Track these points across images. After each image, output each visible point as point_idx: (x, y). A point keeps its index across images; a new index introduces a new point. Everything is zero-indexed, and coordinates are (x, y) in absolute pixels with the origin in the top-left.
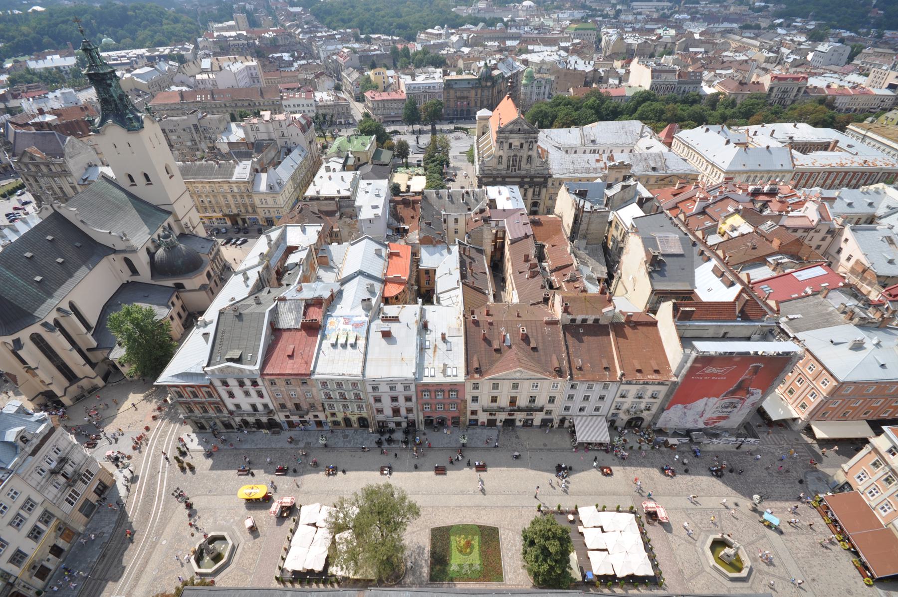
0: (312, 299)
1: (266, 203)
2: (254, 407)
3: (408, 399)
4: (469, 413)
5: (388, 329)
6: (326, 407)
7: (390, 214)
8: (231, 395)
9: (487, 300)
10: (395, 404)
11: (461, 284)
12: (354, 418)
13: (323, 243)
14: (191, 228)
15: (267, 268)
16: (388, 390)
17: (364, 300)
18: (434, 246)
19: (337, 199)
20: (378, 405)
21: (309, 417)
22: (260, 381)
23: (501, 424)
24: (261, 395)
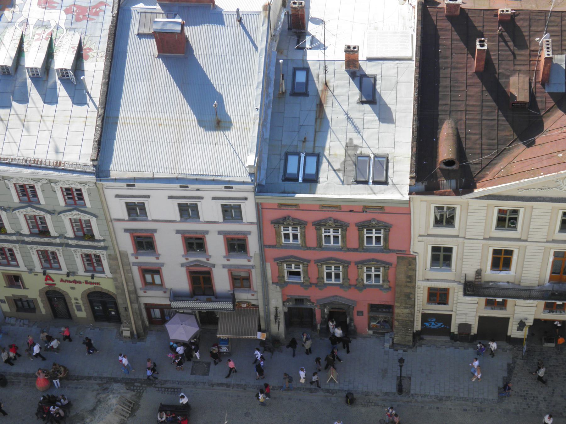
4: (421, 296)
20: (147, 259)
23: (523, 334)
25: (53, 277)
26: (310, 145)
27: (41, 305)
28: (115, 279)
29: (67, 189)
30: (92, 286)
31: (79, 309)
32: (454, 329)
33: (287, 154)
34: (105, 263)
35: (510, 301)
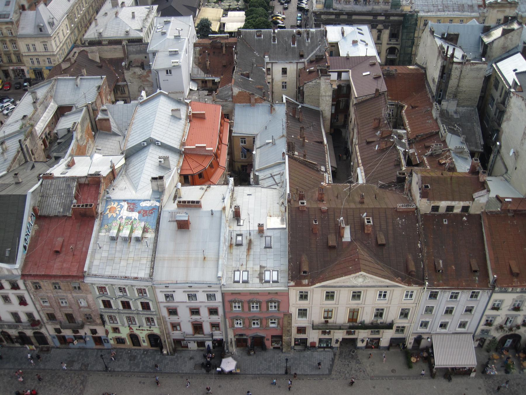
0: (86, 177)
1: (35, 49)
3: (213, 311)
4: (294, 331)
5: (186, 219)
6: (106, 319)
7: (194, 62)
9: (323, 179)
10: (195, 317)
11: (287, 157)
12: (142, 335)
13: (104, 101)
16: (186, 299)
17: (154, 179)
19: (124, 43)
20: (174, 319)
21: (85, 331)
22: (21, 283)
23: (338, 345)
25: (133, 328)
27: (127, 340)
28: (160, 328)
29: (139, 289)
32: (308, 344)
33: (234, 271)
34: (156, 321)
35: (332, 331)
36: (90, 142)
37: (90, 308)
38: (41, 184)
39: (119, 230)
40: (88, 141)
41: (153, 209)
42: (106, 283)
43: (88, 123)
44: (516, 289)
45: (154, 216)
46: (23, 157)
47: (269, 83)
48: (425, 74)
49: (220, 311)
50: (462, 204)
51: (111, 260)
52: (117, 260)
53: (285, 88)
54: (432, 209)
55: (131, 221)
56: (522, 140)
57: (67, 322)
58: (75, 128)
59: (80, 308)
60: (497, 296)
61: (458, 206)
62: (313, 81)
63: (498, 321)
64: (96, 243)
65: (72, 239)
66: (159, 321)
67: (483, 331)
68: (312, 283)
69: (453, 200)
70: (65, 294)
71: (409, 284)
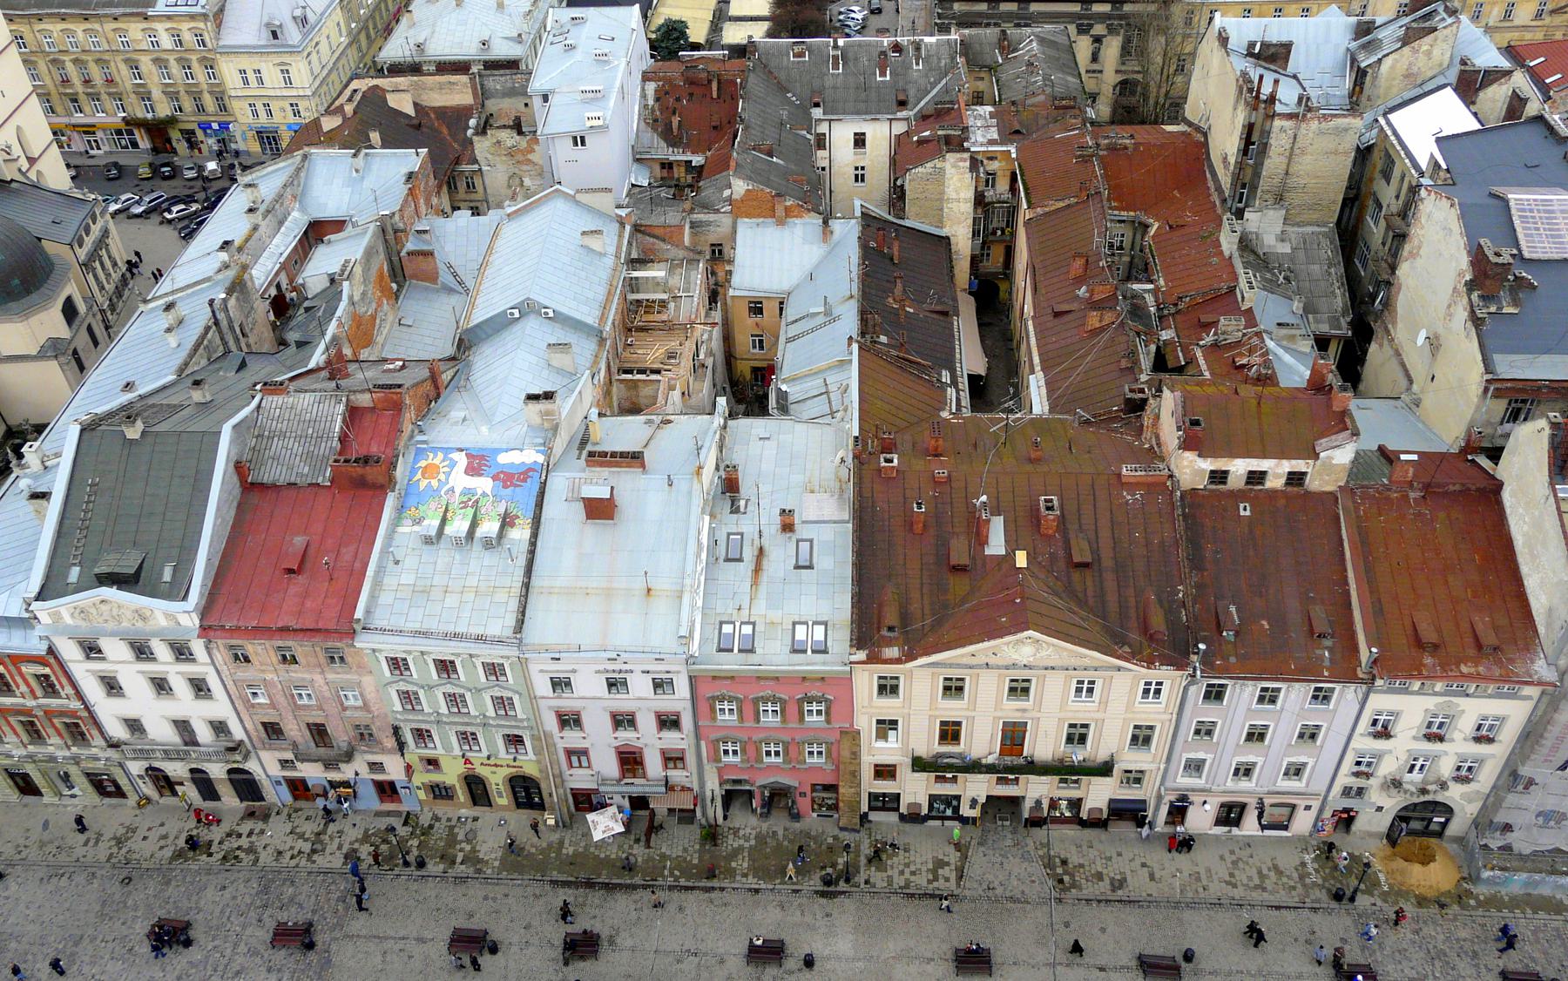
1: (260, 81)
2: (183, 726)
4: (867, 773)
6: (409, 737)
8: (112, 686)
9: (942, 403)
10: (626, 736)
11: (855, 347)
12: (496, 779)
13: (423, 208)
14: (25, 165)
15: (238, 286)
17: (532, 398)
18: (781, 223)
19: (474, 69)
20: (572, 738)
22: (198, 647)
24: (200, 688)
26: (745, 613)
27: (459, 792)
28: (538, 762)
30: (514, 770)
31: (500, 795)
32: (903, 810)
34: (528, 743)
36: (386, 307)
37: (369, 711)
38: (259, 406)
39: (444, 521)
40: (380, 305)
41: (526, 473)
42: (408, 648)
43: (380, 261)
44: (1434, 686)
45: (532, 486)
46: (218, 341)
47: (823, 169)
48: (1206, 144)
49: (687, 721)
50: (1287, 466)
51: (422, 592)
52: (436, 594)
53: (863, 180)
54: (1210, 477)
55: (474, 499)
56: (1449, 306)
57: (313, 744)
58: (347, 273)
59: (345, 709)
60: (1381, 702)
61: (1277, 470)
62: (928, 165)
63: (1386, 768)
64: (385, 551)
65: (330, 541)
66: (536, 743)
67: (1347, 792)
68: (910, 657)
69: (1264, 455)
70: (307, 676)
71: (1150, 663)
